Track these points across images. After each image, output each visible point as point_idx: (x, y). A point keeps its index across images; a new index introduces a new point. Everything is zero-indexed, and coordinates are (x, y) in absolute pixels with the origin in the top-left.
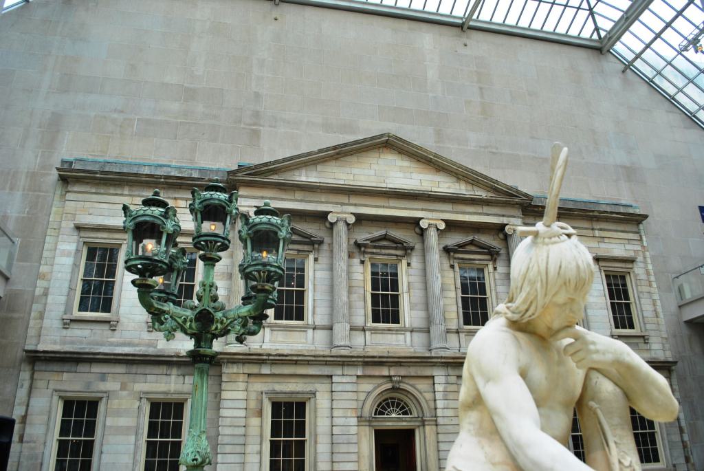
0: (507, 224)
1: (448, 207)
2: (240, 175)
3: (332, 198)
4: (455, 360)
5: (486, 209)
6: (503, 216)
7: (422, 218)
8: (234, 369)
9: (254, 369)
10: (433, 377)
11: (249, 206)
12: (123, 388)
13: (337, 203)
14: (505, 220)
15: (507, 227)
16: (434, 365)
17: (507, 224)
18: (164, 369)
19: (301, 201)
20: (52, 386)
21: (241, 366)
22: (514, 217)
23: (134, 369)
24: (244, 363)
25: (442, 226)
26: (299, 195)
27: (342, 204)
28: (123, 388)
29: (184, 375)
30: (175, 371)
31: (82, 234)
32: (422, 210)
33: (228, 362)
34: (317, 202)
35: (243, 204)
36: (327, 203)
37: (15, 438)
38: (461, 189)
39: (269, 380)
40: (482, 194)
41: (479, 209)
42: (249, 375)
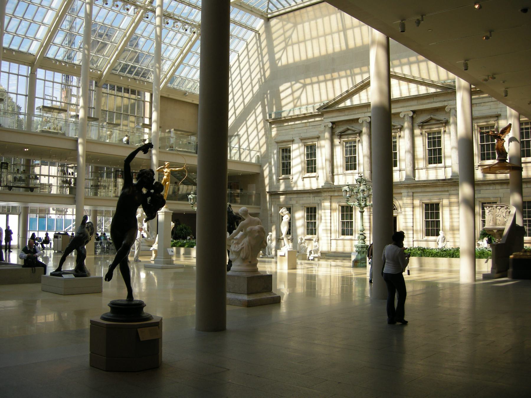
0: (447, 106)
1: (414, 102)
2: (321, 109)
3: (360, 110)
4: (409, 185)
5: (436, 99)
6: (445, 101)
7: (401, 112)
8: (326, 194)
9: (332, 194)
10: (401, 193)
11: (328, 122)
12: (297, 203)
13: (362, 113)
14: (445, 103)
15: (447, 107)
16: (402, 188)
17: (447, 106)
18: (308, 195)
19: (347, 115)
20: (277, 204)
21: (328, 193)
22: (451, 100)
23: (299, 195)
24: (329, 192)
25: (411, 114)
26: (347, 113)
27: (365, 113)
28: (297, 203)
29: (315, 197)
30: (311, 195)
31: (278, 145)
32: (401, 107)
33: (323, 192)
34: (354, 114)
35: (326, 122)
36: (358, 113)
37: (269, 222)
38: (423, 90)
39: (338, 197)
40: (432, 90)
41: (432, 100)
42: (331, 196)
